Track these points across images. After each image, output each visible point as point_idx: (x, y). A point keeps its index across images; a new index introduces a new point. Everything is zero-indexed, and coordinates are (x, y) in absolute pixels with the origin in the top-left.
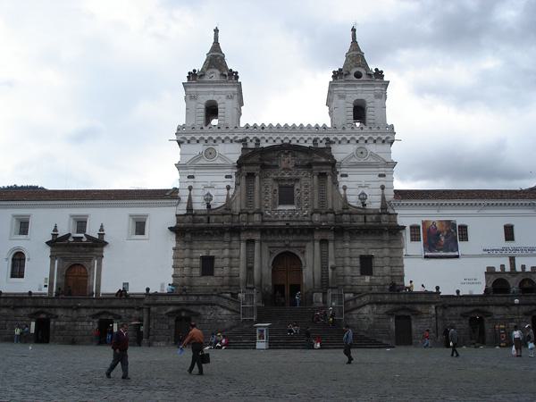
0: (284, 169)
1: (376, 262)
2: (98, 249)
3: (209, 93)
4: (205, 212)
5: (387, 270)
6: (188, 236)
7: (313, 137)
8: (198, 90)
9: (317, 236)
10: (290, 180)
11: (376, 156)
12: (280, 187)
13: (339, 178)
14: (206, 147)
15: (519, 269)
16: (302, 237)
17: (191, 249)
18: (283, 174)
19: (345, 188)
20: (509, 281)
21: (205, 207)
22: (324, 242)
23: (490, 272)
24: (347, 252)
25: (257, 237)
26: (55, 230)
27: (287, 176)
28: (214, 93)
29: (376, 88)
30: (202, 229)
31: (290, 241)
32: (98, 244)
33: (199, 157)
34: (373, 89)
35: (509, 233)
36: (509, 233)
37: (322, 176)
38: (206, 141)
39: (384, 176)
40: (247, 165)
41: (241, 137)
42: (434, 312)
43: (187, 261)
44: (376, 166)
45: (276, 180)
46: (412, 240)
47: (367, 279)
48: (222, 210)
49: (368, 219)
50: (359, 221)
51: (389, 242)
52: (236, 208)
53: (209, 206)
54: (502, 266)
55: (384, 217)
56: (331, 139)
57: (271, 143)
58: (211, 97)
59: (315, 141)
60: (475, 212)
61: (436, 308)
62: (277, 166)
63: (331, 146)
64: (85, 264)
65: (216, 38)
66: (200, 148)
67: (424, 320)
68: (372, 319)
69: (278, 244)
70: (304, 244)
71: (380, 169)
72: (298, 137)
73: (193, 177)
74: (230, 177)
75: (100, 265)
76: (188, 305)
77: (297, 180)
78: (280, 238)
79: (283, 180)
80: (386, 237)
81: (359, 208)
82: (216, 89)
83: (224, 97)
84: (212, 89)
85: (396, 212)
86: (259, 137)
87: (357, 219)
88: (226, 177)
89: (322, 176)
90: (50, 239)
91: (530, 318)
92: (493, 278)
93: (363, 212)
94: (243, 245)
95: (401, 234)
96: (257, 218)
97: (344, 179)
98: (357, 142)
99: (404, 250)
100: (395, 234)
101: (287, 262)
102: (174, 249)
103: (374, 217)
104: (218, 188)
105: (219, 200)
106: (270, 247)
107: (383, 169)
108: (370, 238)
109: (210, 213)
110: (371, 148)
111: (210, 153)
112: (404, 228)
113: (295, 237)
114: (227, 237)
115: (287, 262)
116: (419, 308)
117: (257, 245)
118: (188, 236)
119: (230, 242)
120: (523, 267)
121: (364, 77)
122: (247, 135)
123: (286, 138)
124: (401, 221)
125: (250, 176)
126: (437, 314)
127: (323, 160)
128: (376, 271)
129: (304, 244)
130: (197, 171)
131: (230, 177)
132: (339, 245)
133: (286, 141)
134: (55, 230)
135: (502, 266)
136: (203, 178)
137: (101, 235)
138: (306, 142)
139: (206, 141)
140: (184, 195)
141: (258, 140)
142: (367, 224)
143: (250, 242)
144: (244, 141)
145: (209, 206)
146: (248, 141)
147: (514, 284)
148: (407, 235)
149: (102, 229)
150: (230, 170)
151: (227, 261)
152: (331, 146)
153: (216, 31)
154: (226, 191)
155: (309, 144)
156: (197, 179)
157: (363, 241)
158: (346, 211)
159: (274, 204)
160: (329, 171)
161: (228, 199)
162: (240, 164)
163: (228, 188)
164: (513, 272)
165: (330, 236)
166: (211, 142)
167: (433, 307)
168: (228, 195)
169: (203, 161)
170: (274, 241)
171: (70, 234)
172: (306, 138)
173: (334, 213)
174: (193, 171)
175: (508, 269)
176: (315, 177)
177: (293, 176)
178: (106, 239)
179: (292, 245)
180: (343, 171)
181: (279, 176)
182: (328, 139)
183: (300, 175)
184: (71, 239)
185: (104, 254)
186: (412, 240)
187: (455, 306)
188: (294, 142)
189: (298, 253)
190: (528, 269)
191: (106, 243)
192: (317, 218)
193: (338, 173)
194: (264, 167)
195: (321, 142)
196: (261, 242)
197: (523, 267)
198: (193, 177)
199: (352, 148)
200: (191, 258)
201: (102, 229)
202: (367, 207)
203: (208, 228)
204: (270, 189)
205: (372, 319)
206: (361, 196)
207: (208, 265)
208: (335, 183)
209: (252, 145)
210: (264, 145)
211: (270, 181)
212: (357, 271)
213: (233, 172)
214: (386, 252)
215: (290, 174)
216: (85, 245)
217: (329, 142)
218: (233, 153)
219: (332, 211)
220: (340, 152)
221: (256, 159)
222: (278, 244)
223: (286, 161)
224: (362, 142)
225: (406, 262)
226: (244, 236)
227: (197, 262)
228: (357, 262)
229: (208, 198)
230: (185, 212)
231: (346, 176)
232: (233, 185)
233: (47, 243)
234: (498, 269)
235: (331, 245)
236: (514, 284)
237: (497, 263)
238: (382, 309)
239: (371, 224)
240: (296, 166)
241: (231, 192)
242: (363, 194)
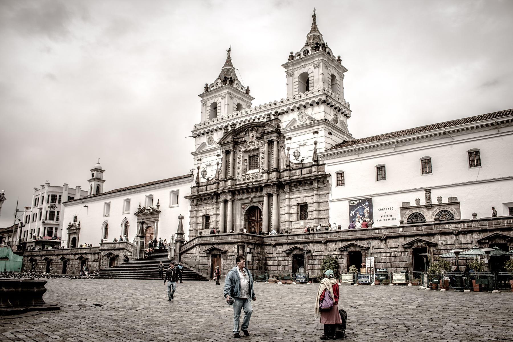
0: (250, 142)
1: (310, 209)
2: (155, 216)
3: (212, 98)
4: (205, 184)
5: (315, 214)
6: (195, 201)
7: (267, 113)
8: (207, 97)
9: (265, 192)
10: (253, 150)
11: (310, 118)
12: (251, 157)
13: (286, 142)
14: (208, 137)
15: (434, 201)
16: (259, 194)
17: (197, 211)
18: (249, 147)
19: (289, 149)
20: (424, 215)
21: (205, 180)
22: (270, 196)
23: (405, 207)
24: (287, 202)
25: (229, 197)
26: (140, 206)
27: (251, 148)
28: (215, 97)
29: (315, 60)
30: (205, 195)
31: (252, 198)
32: (156, 212)
33: (203, 145)
34: (312, 61)
35: (426, 166)
36: (426, 166)
37: (270, 143)
38: (207, 133)
39: (316, 133)
40: (225, 144)
41: (224, 125)
42: (236, 250)
43: (194, 219)
44: (310, 126)
45: (245, 152)
46: (338, 185)
47: (302, 223)
48: (214, 180)
49: (303, 173)
50: (297, 175)
51: (318, 189)
52: (220, 178)
53: (208, 179)
54: (418, 201)
55: (314, 169)
56: (279, 111)
57: (243, 124)
58: (212, 101)
59: (269, 115)
60: (392, 150)
61: (238, 246)
62: (245, 141)
63: (279, 117)
64: (152, 225)
65: (229, 56)
66: (204, 139)
67: (230, 257)
68: (198, 257)
69: (247, 201)
70: (261, 199)
71: (314, 128)
72: (258, 116)
73: (200, 160)
74: (219, 155)
75: (157, 225)
76: (115, 250)
77: (258, 149)
78: (245, 196)
79: (249, 151)
80: (315, 185)
81: (299, 164)
82: (216, 94)
83: (220, 98)
84: (214, 95)
85: (325, 162)
86: (235, 122)
87: (295, 173)
88: (217, 156)
89: (270, 143)
90: (138, 210)
91: (346, 253)
92: (408, 213)
93: (301, 166)
94: (221, 205)
95: (328, 181)
96: (229, 183)
97: (289, 141)
98: (298, 108)
99: (330, 195)
100: (323, 182)
101: (253, 214)
102: (190, 212)
103: (307, 170)
104: (212, 165)
105: (211, 174)
106: (243, 204)
107: (317, 127)
108: (305, 188)
109: (209, 183)
110: (310, 111)
111: (210, 141)
112: (330, 175)
113: (254, 195)
114: (214, 201)
115: (253, 214)
116: (226, 248)
117: (230, 203)
118: (195, 201)
119: (217, 203)
120: (440, 199)
121: (310, 53)
122: (228, 122)
123: (251, 118)
124: (328, 170)
125: (227, 153)
126: (238, 252)
127: (271, 129)
128: (310, 216)
129: (261, 199)
130: (202, 155)
131: (219, 155)
132: (282, 197)
133: (252, 121)
134: (140, 206)
135: (418, 201)
136: (207, 159)
137: (158, 206)
138: (264, 118)
139: (207, 133)
140: (195, 172)
141: (234, 125)
142: (303, 176)
143: (226, 202)
144: (227, 127)
145: (208, 179)
146: (229, 127)
147: (430, 217)
148: (333, 180)
149: (158, 203)
150: (219, 151)
151: (215, 216)
152: (279, 117)
153: (229, 51)
154: (216, 166)
155: (265, 120)
156: (203, 160)
157: (300, 192)
158: (288, 168)
159: (244, 171)
160: (274, 138)
161: (218, 173)
162: (222, 143)
163: (218, 164)
164: (429, 206)
165: (273, 191)
166: (210, 133)
167: (236, 246)
168: (217, 169)
169: (208, 147)
170: (242, 199)
171: (144, 208)
172: (263, 115)
173: (280, 172)
174: (200, 156)
175: (423, 202)
176: (266, 145)
177: (256, 147)
178: (160, 209)
179: (255, 200)
180: (287, 135)
181: (247, 148)
182: (276, 112)
183: (260, 145)
184: (146, 211)
185: (159, 219)
186: (338, 185)
187: (281, 244)
188: (257, 120)
189: (259, 206)
190: (445, 201)
191: (159, 212)
192: (265, 176)
193: (284, 137)
194: (236, 144)
195: (274, 115)
196: (233, 201)
197: (440, 199)
198: (200, 160)
199: (295, 115)
200: (197, 217)
201: (158, 203)
202: (304, 162)
203: (208, 194)
204: (241, 159)
205: (198, 257)
206: (296, 154)
207: (207, 218)
208: (283, 147)
209: (230, 129)
210: (238, 126)
211: (241, 154)
212: (294, 218)
213: (220, 151)
214: (315, 199)
215: (253, 146)
216: (151, 214)
217: (277, 114)
218: (218, 136)
219: (277, 170)
220: (285, 121)
221: (230, 139)
222: (247, 201)
223: (251, 136)
224: (302, 108)
225: (332, 206)
226: (223, 198)
227: (200, 220)
228: (294, 210)
229: (204, 174)
230: (196, 185)
231: (289, 139)
232: (220, 162)
233: (135, 214)
234: (413, 204)
235: (275, 198)
236: (430, 217)
237: (411, 199)
238: (204, 248)
239: (305, 176)
240: (257, 138)
241: (219, 167)
242: (297, 151)
